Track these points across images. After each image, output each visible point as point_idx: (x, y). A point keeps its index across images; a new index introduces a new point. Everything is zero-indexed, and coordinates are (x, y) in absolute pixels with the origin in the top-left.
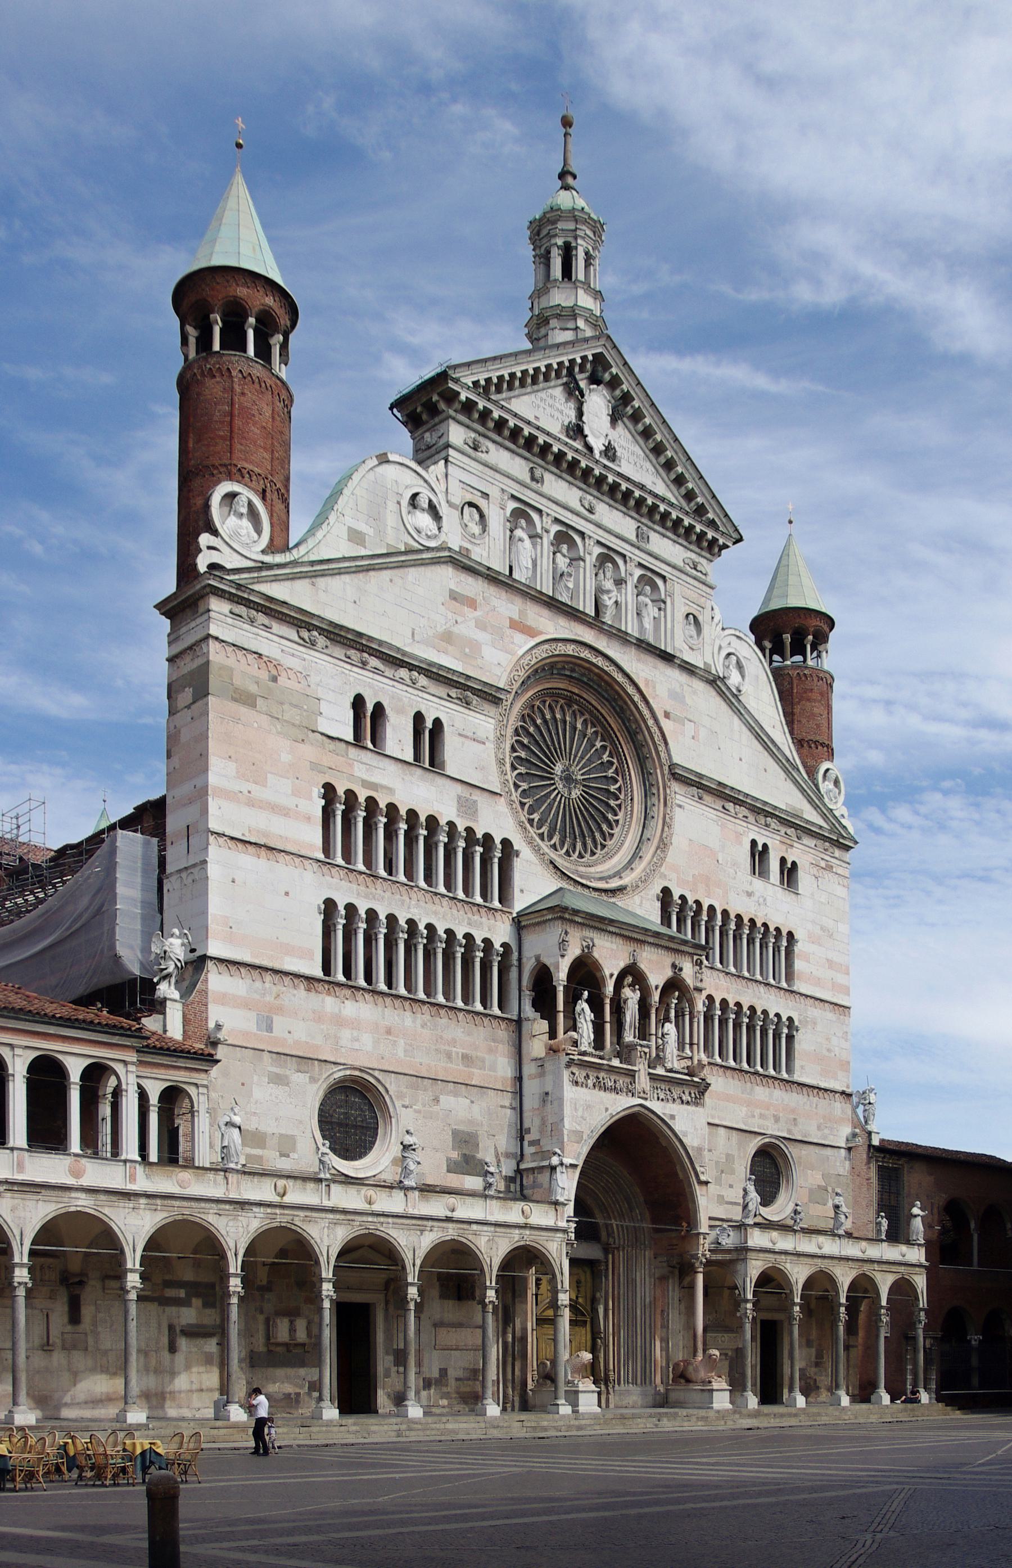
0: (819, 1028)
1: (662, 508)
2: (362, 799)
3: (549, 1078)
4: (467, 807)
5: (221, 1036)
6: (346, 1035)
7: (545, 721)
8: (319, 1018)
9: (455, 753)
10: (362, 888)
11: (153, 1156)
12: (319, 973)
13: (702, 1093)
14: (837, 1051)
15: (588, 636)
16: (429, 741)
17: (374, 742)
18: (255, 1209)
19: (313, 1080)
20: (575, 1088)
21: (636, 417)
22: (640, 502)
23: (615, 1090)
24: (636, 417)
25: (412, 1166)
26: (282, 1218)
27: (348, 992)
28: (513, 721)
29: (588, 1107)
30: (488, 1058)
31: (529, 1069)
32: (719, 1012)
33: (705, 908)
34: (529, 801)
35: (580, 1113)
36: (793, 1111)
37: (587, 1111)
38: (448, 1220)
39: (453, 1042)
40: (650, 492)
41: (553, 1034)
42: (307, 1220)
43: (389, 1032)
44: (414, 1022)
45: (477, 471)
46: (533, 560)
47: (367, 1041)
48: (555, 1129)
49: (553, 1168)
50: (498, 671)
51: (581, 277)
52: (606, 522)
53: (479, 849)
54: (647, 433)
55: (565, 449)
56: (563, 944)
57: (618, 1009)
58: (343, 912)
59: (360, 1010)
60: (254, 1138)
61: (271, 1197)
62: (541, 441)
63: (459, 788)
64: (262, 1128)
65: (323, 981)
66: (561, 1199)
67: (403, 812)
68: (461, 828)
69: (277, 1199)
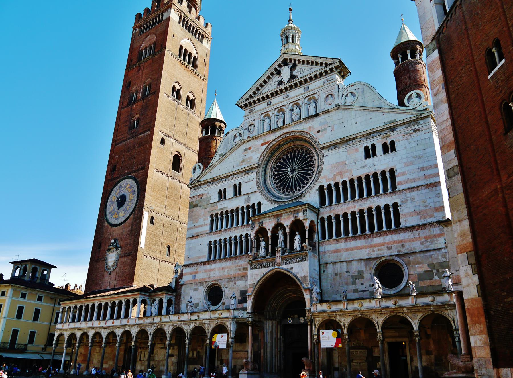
6: (212, 273)
8: (206, 271)
20: (252, 270)
29: (257, 275)
35: (253, 278)
38: (196, 320)
39: (241, 265)
43: (223, 269)
59: (217, 266)
63: (245, 197)
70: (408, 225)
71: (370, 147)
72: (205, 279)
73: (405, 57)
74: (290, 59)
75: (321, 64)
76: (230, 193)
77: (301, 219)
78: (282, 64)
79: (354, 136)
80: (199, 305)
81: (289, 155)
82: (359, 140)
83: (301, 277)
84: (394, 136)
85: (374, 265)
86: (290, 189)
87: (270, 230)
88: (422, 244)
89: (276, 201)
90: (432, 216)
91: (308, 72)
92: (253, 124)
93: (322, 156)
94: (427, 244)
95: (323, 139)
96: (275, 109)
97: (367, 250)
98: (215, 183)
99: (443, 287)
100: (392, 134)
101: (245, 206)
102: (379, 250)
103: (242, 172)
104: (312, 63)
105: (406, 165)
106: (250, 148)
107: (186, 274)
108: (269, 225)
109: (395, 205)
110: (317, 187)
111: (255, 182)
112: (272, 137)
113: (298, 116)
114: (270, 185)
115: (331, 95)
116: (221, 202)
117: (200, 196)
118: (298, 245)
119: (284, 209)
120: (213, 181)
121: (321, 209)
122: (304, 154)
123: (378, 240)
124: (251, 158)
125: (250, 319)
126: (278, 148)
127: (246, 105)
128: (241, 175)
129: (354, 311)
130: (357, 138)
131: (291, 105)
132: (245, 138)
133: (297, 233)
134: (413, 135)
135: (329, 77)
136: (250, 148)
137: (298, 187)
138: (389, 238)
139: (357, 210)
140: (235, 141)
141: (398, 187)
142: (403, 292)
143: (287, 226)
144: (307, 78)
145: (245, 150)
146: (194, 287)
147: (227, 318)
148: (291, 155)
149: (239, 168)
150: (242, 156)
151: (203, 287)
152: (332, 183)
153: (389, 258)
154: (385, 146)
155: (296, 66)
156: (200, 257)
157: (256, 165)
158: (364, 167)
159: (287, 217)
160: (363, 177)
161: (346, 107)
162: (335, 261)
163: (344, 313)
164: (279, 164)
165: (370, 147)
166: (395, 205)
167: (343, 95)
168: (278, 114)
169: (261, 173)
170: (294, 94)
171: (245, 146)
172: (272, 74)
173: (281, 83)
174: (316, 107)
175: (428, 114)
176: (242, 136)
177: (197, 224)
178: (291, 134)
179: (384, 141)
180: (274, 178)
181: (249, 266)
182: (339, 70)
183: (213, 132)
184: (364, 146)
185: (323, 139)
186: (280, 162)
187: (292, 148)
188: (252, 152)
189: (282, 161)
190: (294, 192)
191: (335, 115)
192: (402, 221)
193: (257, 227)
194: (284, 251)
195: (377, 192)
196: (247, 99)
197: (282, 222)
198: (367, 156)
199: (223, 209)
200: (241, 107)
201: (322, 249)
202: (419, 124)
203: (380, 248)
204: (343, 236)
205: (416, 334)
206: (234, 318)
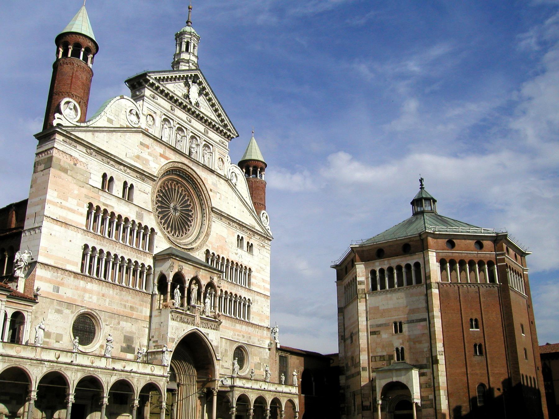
0: (259, 304)
1: (213, 123)
2: (102, 209)
3: (163, 317)
4: (140, 216)
5: (38, 293)
6: (87, 296)
7: (169, 189)
8: (77, 288)
9: (137, 196)
10: (99, 241)
11: (6, 340)
12: (79, 272)
13: (219, 325)
14: (265, 312)
15: (186, 161)
16: (128, 189)
17: (108, 190)
18: (46, 363)
19: (72, 312)
20: (173, 321)
21: (207, 95)
22: (206, 121)
23: (188, 323)
24: (207, 95)
25: (110, 349)
26: (56, 368)
27: (89, 279)
28: (158, 188)
29: (177, 329)
30: (140, 308)
31: (155, 313)
32: (224, 296)
33: (221, 258)
34: (161, 216)
36: (249, 334)
37: (177, 330)
38: (122, 371)
39: (127, 301)
40: (210, 118)
41: (165, 300)
42: (66, 369)
44: (113, 291)
45: (152, 104)
46: (168, 135)
47: (95, 298)
48: (164, 337)
49: (163, 352)
50: (154, 170)
51: (192, 51)
53: (143, 231)
54: (210, 100)
55: (183, 102)
56: (171, 267)
57: (189, 292)
58: (91, 250)
59: (93, 286)
60: (48, 335)
61: (53, 358)
62: (175, 98)
63: (137, 209)
64: (50, 330)
65: (80, 275)
66: (166, 365)
67: (116, 215)
68: (137, 223)
69: (56, 360)
72: (75, 300)
75: (222, 121)
76: (117, 188)
80: (64, 338)
85: (235, 346)
90: (264, 321)
92: (152, 117)
94: (261, 342)
95: (216, 202)
96: (178, 123)
97: (232, 332)
98: (100, 157)
106: (148, 147)
110: (204, 250)
122: (186, 198)
127: (152, 85)
128: (135, 174)
137: (177, 233)
145: (141, 144)
146: (56, 305)
150: (137, 148)
151: (72, 312)
156: (69, 262)
158: (236, 254)
159: (204, 274)
176: (141, 120)
177: (64, 203)
178: (189, 170)
186: (164, 188)
188: (150, 154)
192: (251, 316)
193: (176, 270)
196: (156, 78)
197: (200, 277)
199: (107, 205)
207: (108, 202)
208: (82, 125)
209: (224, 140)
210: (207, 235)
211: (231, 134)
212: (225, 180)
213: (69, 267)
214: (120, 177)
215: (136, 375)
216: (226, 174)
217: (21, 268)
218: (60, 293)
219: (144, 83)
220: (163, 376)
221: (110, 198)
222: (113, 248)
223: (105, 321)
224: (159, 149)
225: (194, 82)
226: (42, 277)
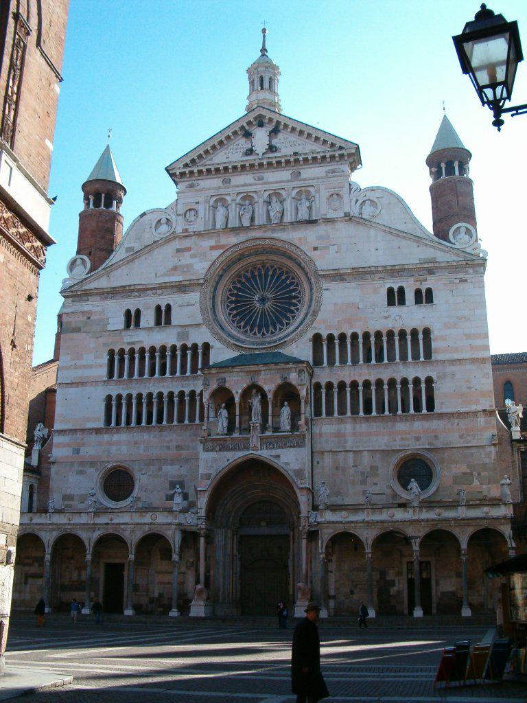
4: (180, 337)
6: (114, 448)
35: (209, 465)
38: (107, 524)
39: (171, 440)
47: (124, 449)
52: (271, 179)
59: (122, 437)
63: (179, 330)
64: (72, 493)
68: (179, 345)
70: (445, 410)
71: (396, 290)
73: (450, 171)
74: (271, 120)
75: (325, 142)
76: (148, 319)
77: (294, 383)
78: (254, 123)
79: (373, 269)
81: (256, 273)
82: (381, 275)
83: (294, 471)
84: (431, 282)
85: (395, 459)
86: (256, 329)
87: (239, 394)
88: (461, 437)
89: (237, 345)
90: (477, 402)
91: (299, 149)
93: (320, 290)
94: (469, 438)
96: (238, 194)
97: (386, 438)
99: (484, 494)
100: (429, 278)
101: (179, 345)
102: (402, 439)
103: (172, 287)
104: (309, 135)
105: (447, 326)
106: (189, 249)
107: (59, 445)
108: (237, 383)
109: (429, 381)
110: (310, 335)
111: (198, 305)
112: (233, 240)
113: (279, 215)
114: (222, 317)
115: (337, 194)
116: (130, 333)
117: (88, 315)
118: (287, 422)
119: (265, 364)
120: (115, 292)
121: (316, 370)
122: (283, 277)
123: (401, 426)
124: (191, 266)
125: (204, 526)
126: (239, 260)
127: (183, 174)
129: (382, 522)
130: (377, 272)
131: (267, 194)
132: (179, 230)
133: (286, 403)
134: (458, 285)
135: (334, 166)
136: (189, 249)
137: (271, 329)
138: (418, 425)
139: (373, 380)
140: (159, 231)
141: (435, 357)
142: (432, 499)
143: (270, 391)
144: (301, 159)
145: (178, 251)
146: (76, 467)
147: (167, 524)
148: (260, 275)
149: (167, 279)
152: (336, 334)
153: (415, 452)
154: (418, 293)
155: (279, 131)
156: (89, 420)
157: (202, 281)
158: (386, 318)
160: (384, 333)
161: (361, 221)
162: (335, 450)
163: (369, 524)
164: (239, 285)
165: (396, 290)
166: (429, 381)
167: (357, 201)
168: (242, 203)
169: (209, 295)
170: (273, 176)
171: (177, 244)
172: (235, 133)
173: (250, 152)
174: (310, 208)
175: (480, 262)
177: (79, 363)
178: (267, 242)
179: (418, 286)
180: (228, 306)
181: (200, 447)
182: (351, 160)
183: (108, 205)
184: (387, 286)
185: (324, 261)
186: (239, 282)
187: (263, 263)
188: (193, 256)
189: (243, 280)
190: (263, 334)
191: (343, 231)
192: (437, 403)
193: (214, 386)
194: (264, 428)
195: (404, 358)
196: (186, 165)
197: (260, 383)
198: (391, 302)
199: (133, 343)
200: (172, 175)
201: (316, 430)
202: (467, 273)
203: (404, 437)
204: (349, 414)
205: (463, 552)
206: (179, 524)
207: (135, 339)
208: (92, 274)
209: (333, 167)
210: (315, 313)
211: (343, 152)
212: (346, 221)
213: (89, 425)
214: (147, 306)
215: (129, 526)
216: (347, 210)
217: (37, 441)
218: (80, 454)
219: (177, 180)
220: (170, 524)
221: (138, 333)
222: (146, 386)
223: (140, 470)
224: (207, 243)
225: (261, 125)
226: (60, 443)
